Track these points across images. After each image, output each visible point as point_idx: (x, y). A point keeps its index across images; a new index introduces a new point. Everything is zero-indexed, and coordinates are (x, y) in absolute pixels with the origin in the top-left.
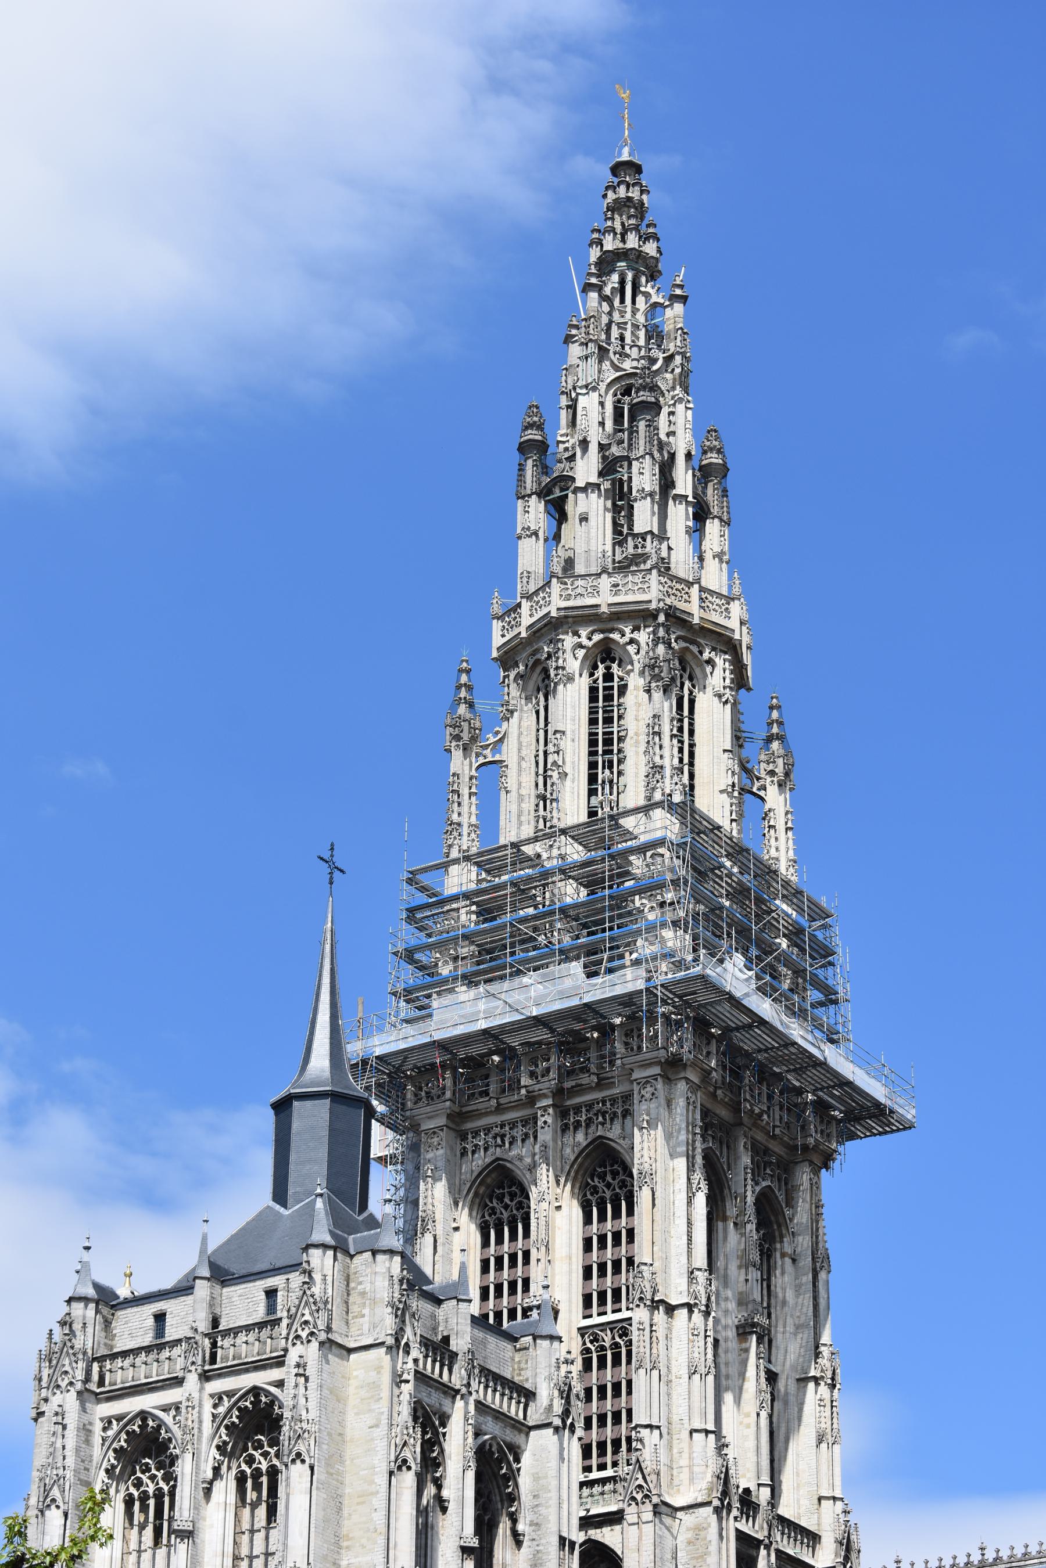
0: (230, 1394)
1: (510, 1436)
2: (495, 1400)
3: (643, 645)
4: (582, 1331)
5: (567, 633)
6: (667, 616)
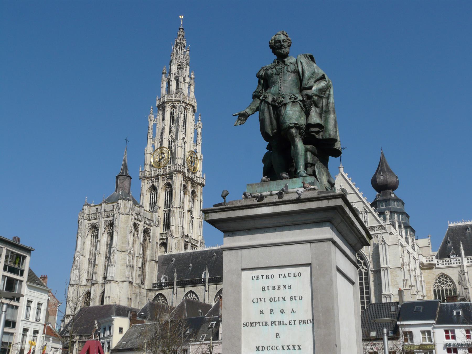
0: (107, 221)
1: (149, 227)
2: (148, 222)
4: (164, 211)
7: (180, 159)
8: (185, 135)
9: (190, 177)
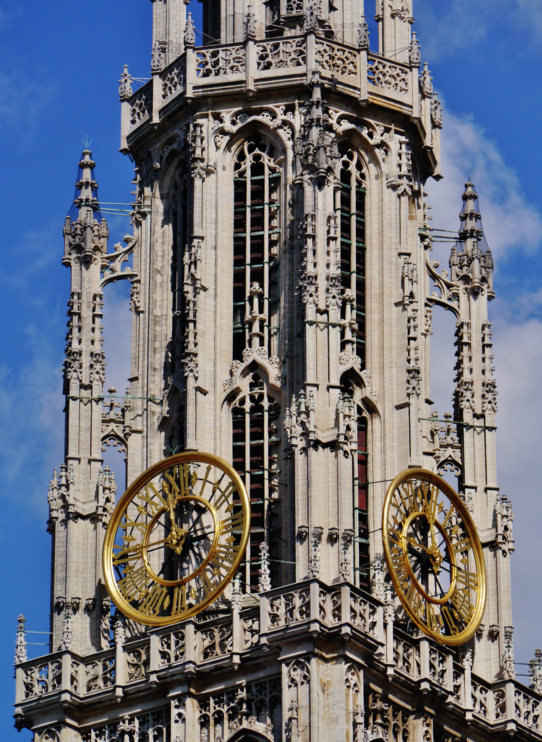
3: (297, 128)
5: (206, 116)
6: (325, 92)
7: (332, 539)
8: (361, 352)
9: (425, 685)
